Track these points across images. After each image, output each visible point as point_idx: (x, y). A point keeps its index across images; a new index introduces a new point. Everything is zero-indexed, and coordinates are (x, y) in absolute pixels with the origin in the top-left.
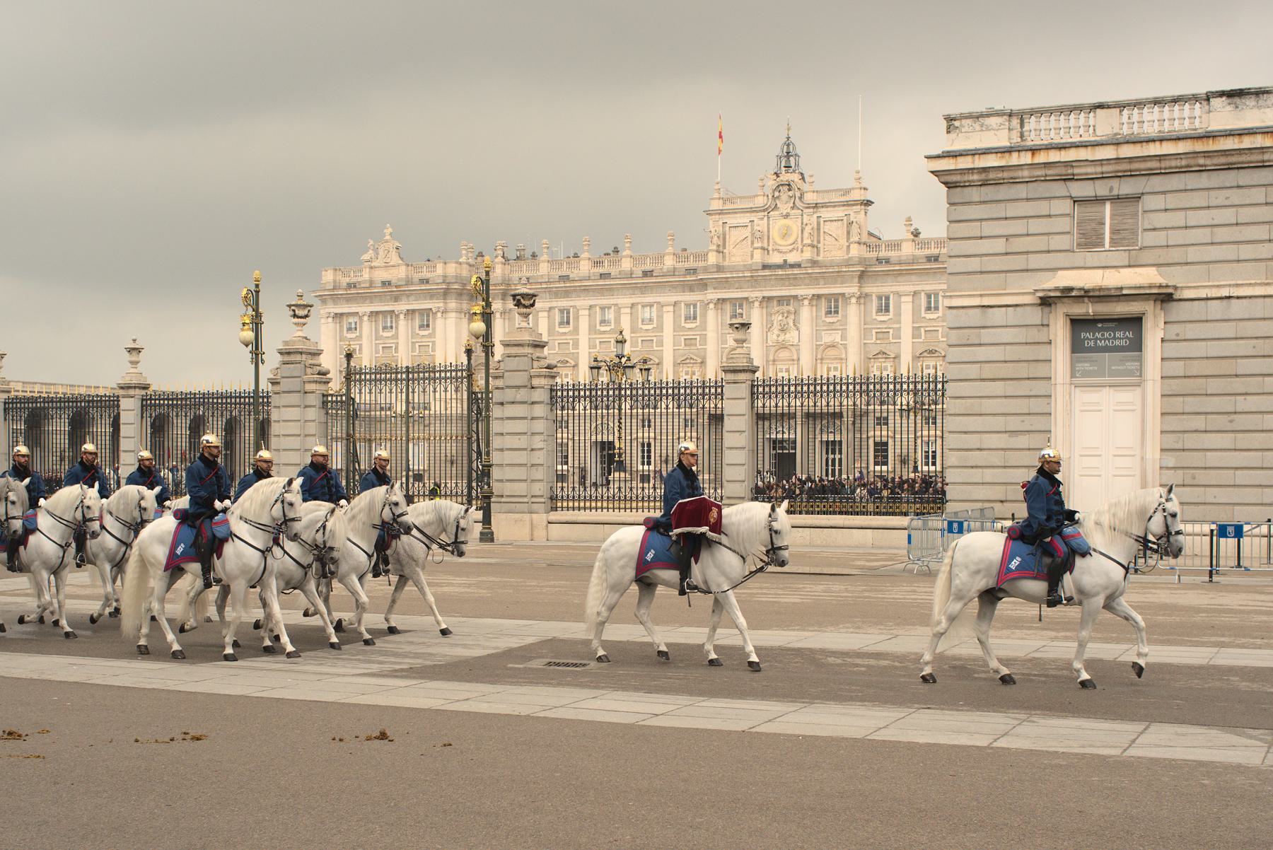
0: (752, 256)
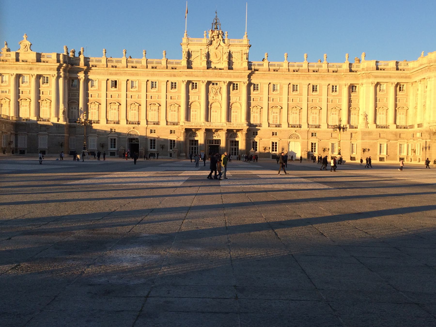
0: (201, 64)
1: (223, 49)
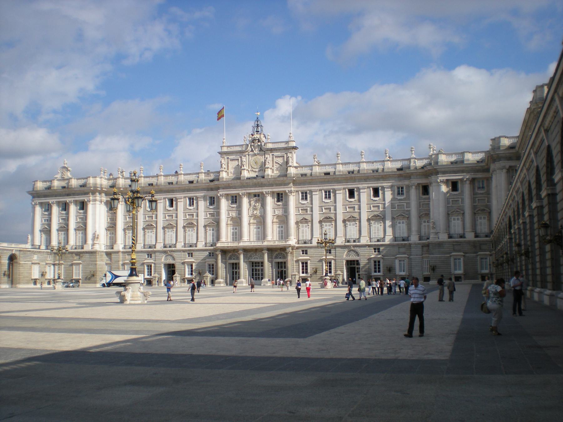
1: (265, 154)
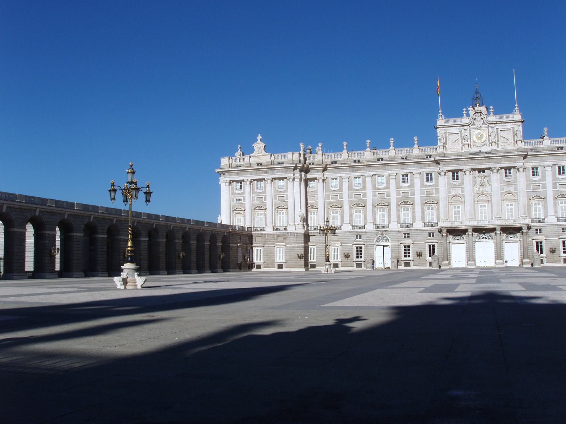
0: (462, 149)
